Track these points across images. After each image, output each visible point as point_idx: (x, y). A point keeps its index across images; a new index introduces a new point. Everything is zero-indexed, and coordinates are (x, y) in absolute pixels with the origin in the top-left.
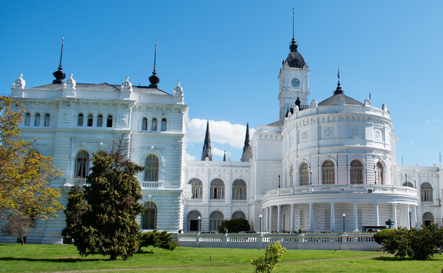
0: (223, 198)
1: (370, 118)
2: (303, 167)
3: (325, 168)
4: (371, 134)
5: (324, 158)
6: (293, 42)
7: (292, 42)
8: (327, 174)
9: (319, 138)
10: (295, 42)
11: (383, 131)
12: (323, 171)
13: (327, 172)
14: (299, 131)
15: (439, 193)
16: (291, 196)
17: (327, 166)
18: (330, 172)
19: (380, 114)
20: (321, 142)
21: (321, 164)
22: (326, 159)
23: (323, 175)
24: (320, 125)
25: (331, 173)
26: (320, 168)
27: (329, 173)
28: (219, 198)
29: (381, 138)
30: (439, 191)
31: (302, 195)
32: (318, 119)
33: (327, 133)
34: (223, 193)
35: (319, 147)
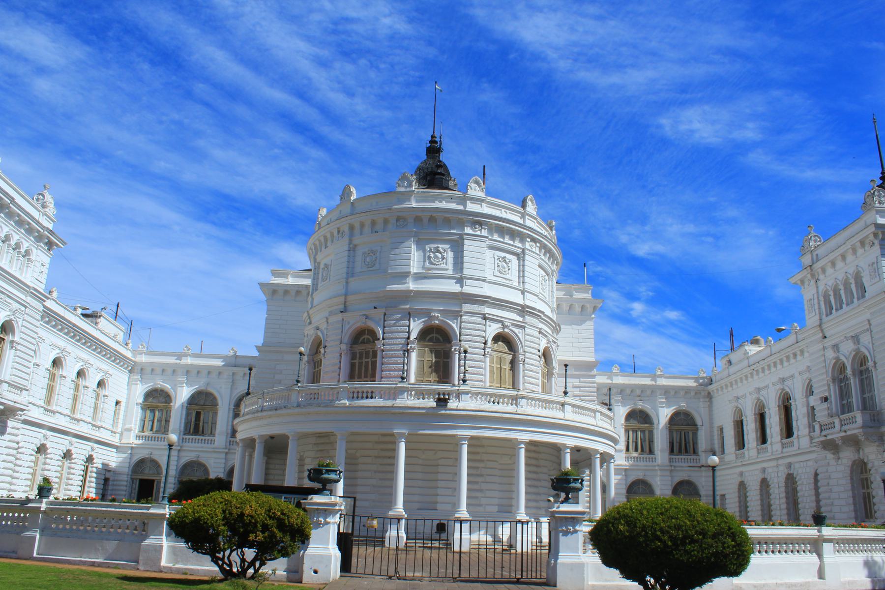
0: (212, 434)
1: (478, 221)
2: (317, 346)
3: (358, 348)
4: (482, 262)
5: (354, 322)
6: (433, 141)
7: (431, 142)
8: (361, 364)
9: (350, 273)
10: (436, 142)
11: (520, 256)
12: (353, 357)
13: (361, 358)
14: (319, 263)
15: (712, 436)
16: (256, 415)
17: (363, 342)
18: (367, 357)
19: (517, 218)
20: (354, 284)
21: (346, 339)
22: (359, 324)
23: (352, 366)
24: (357, 240)
25: (370, 360)
26: (344, 347)
27: (364, 360)
28: (203, 434)
29: (513, 275)
30: (712, 432)
31: (274, 412)
32: (352, 228)
33: (368, 260)
34: (214, 423)
35: (346, 295)
